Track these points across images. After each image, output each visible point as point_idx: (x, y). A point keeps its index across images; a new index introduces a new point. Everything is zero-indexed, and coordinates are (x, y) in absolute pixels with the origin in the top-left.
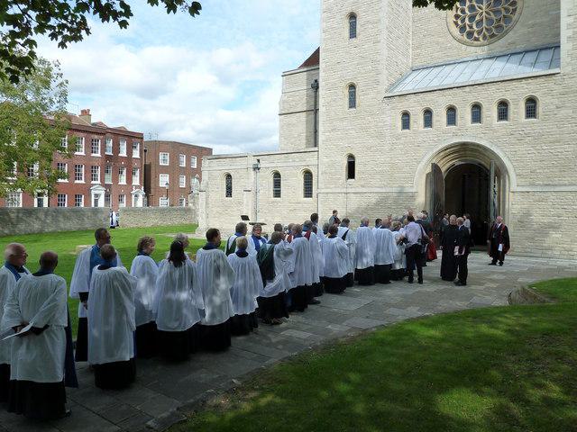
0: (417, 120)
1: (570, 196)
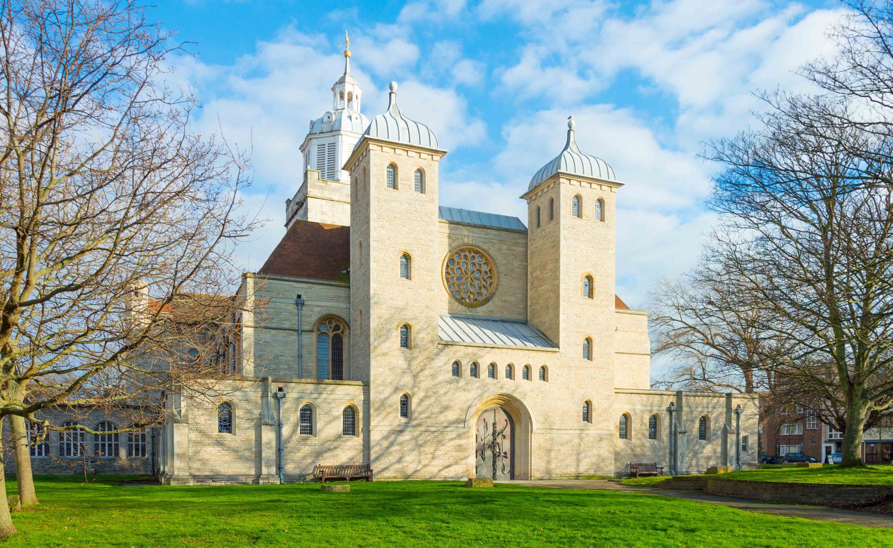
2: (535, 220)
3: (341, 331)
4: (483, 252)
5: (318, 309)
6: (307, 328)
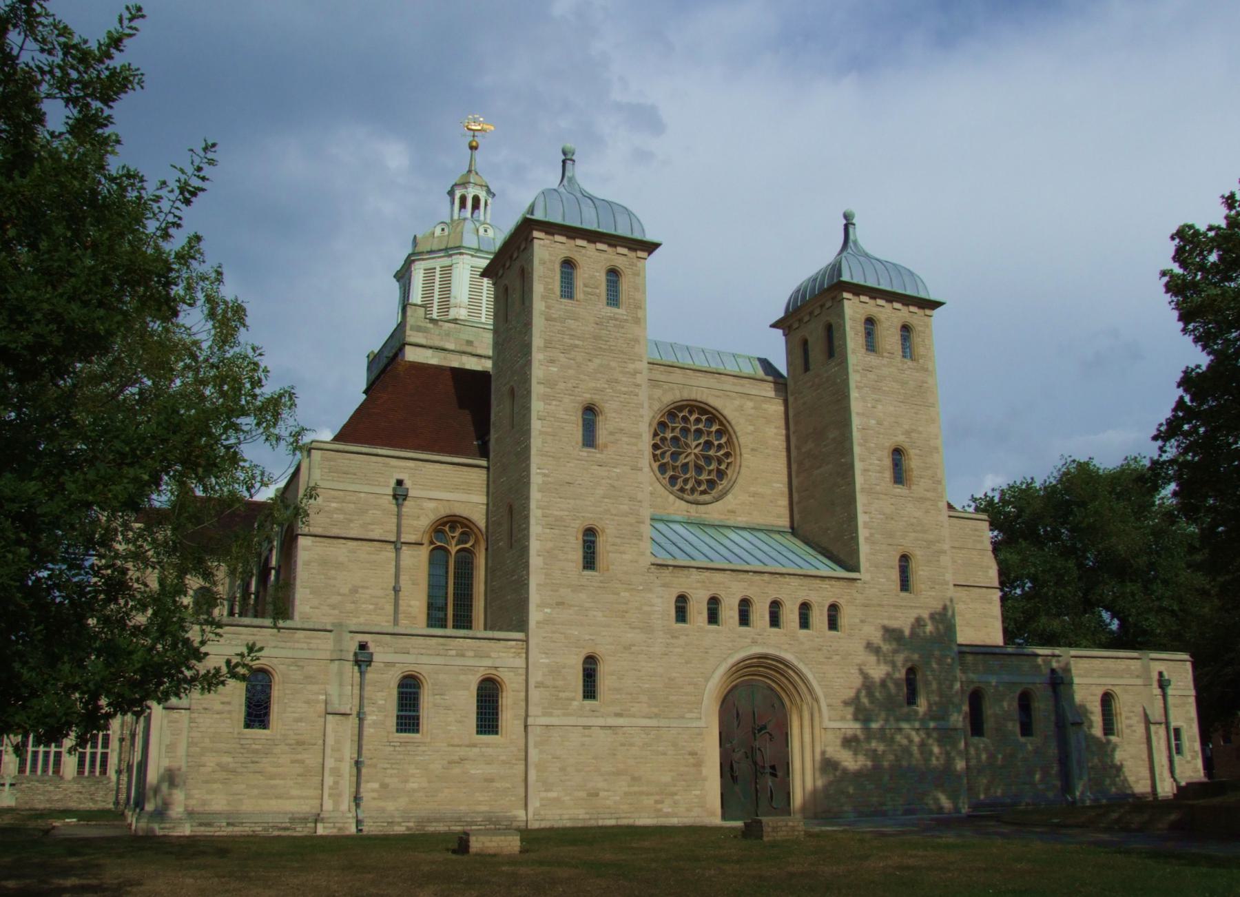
0: (698, 611)
2: (799, 362)
4: (714, 411)
5: (432, 505)
6: (412, 538)
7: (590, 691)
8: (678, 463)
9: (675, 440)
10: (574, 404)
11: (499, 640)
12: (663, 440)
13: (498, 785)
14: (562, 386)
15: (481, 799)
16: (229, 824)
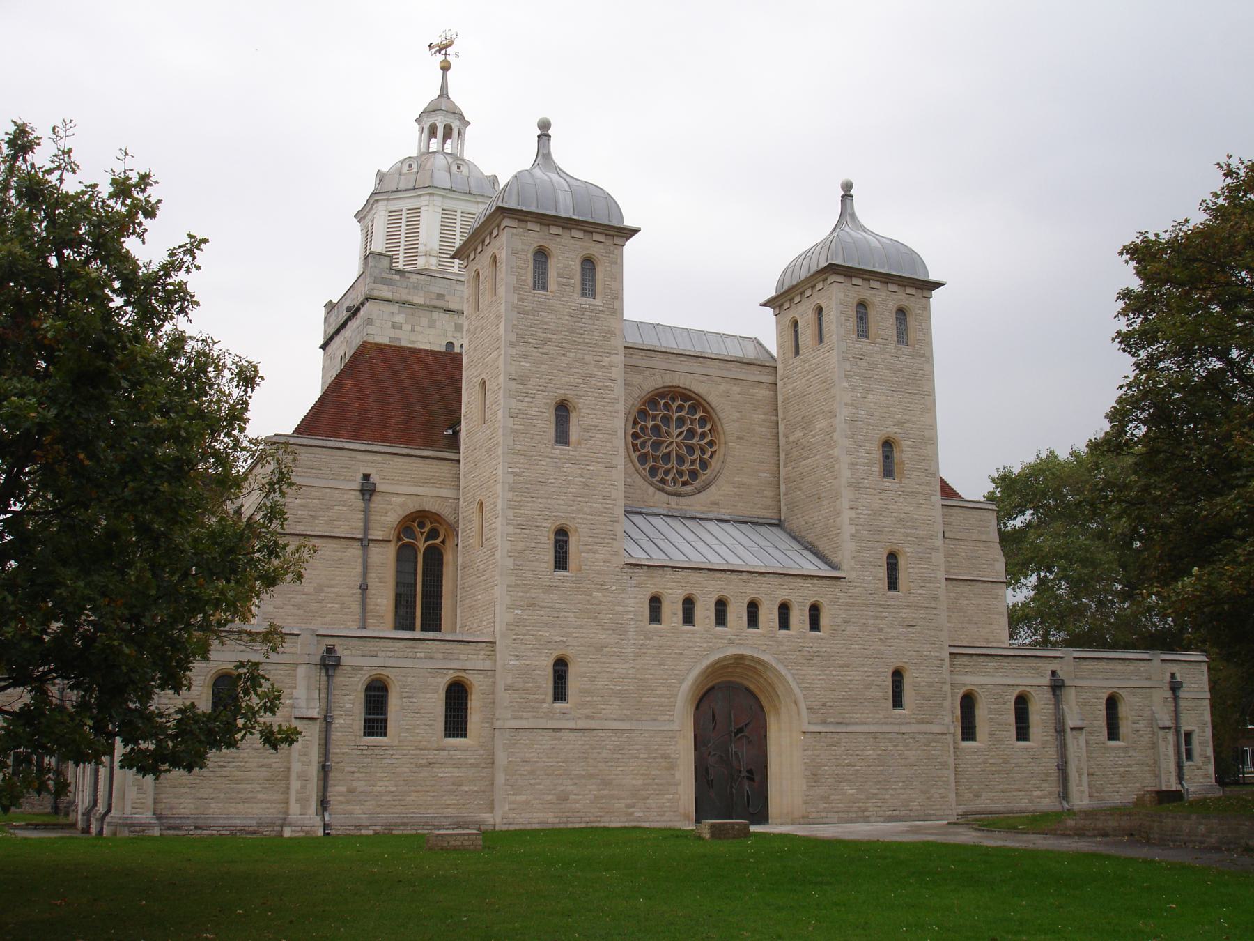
0: (672, 610)
1: (862, 738)
2: (790, 344)
3: (440, 539)
4: (698, 398)
5: (401, 499)
7: (560, 694)
8: (659, 453)
9: (656, 429)
10: (545, 401)
11: (468, 642)
12: (643, 429)
13: (466, 789)
14: (534, 381)
15: (448, 802)
16: (196, 828)
